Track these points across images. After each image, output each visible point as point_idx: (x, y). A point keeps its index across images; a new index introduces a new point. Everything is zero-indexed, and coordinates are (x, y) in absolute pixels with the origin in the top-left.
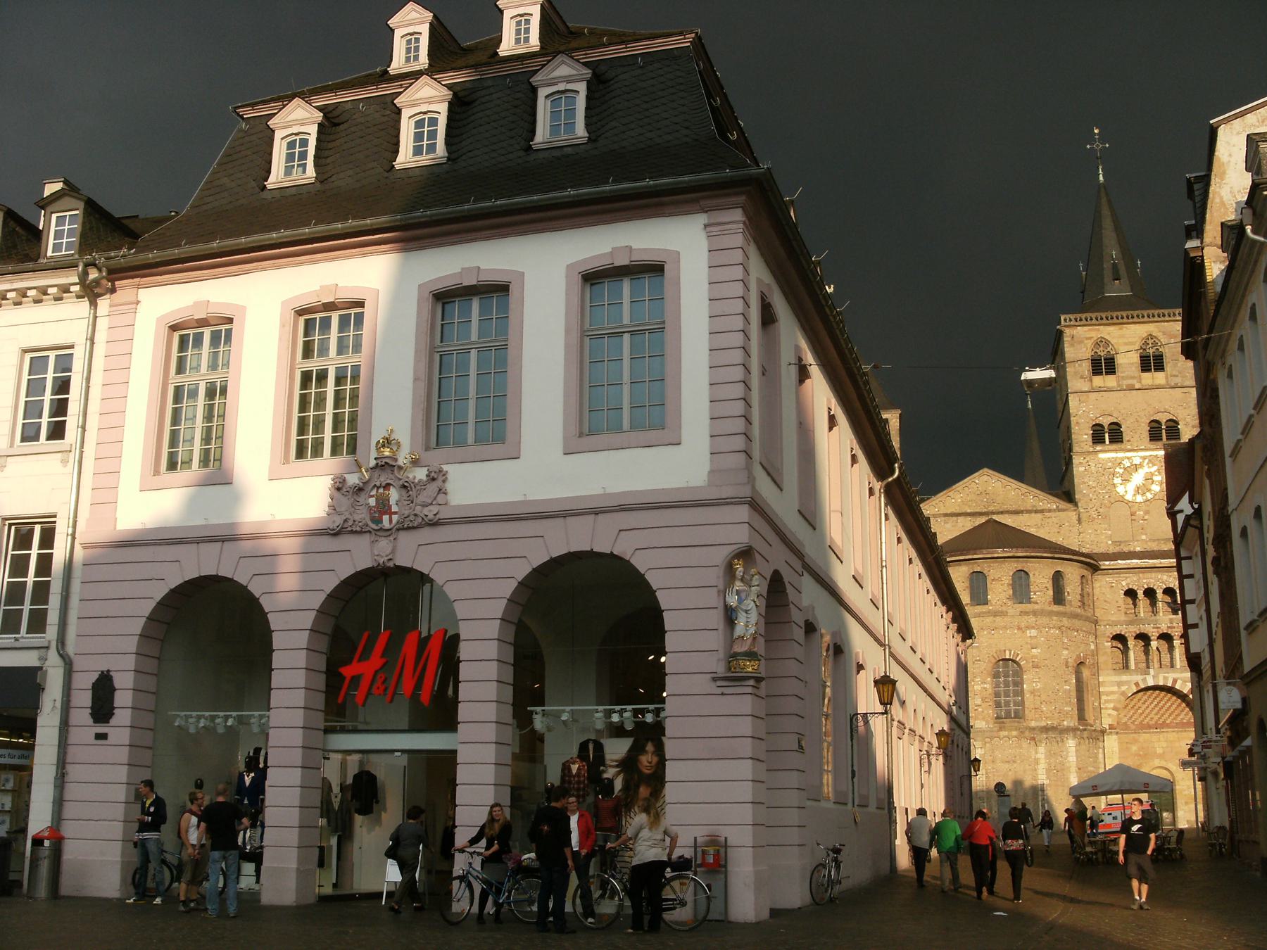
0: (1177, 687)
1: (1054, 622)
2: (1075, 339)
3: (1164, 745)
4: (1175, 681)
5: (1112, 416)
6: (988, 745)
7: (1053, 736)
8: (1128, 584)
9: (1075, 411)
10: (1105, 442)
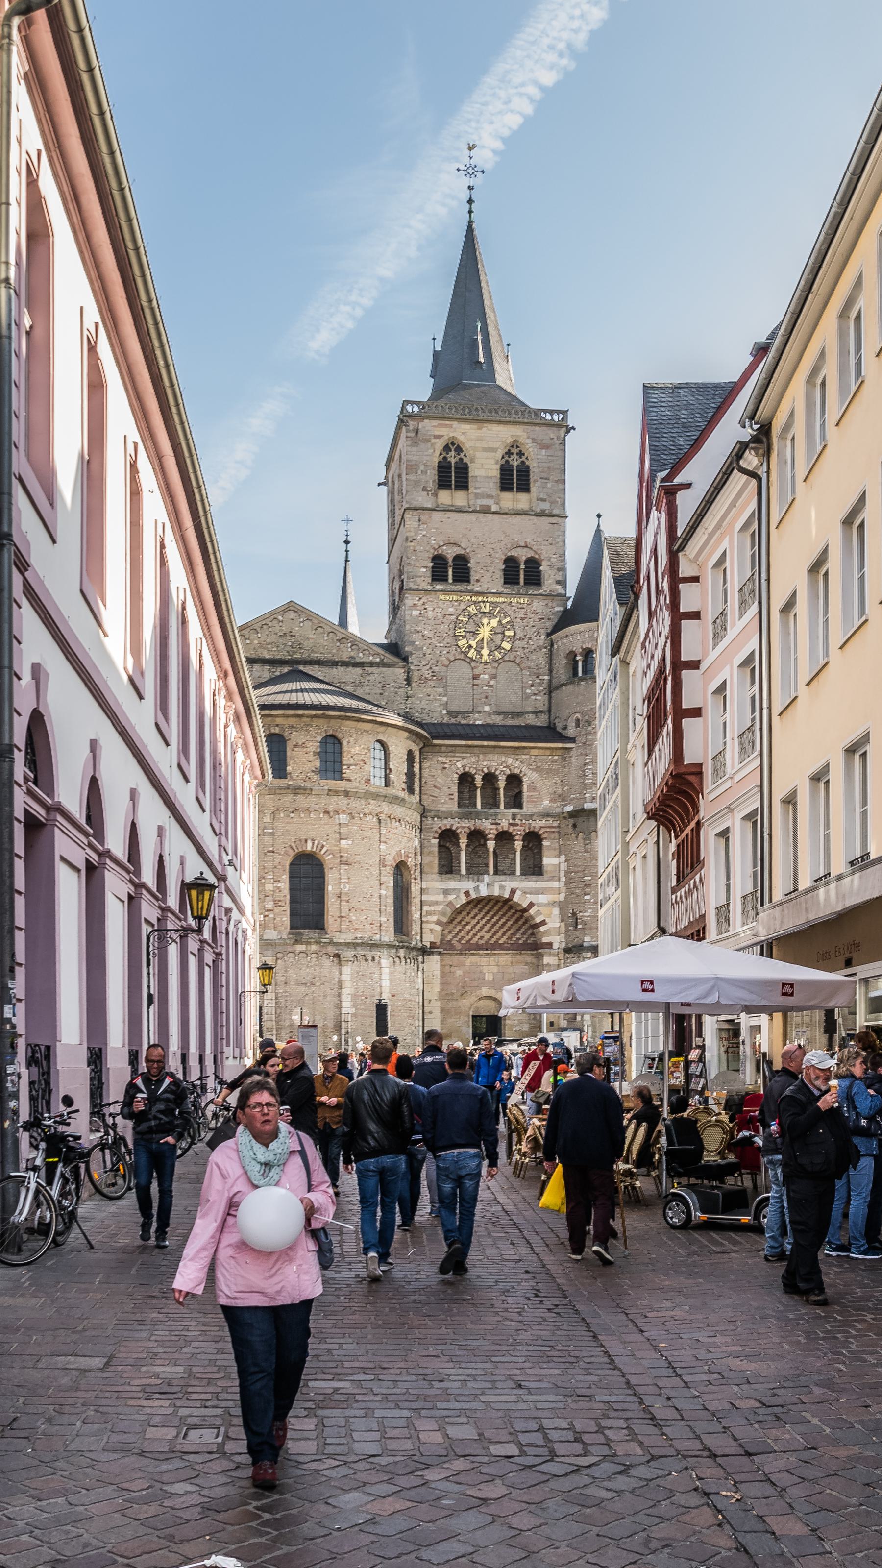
0: (516, 899)
2: (420, 435)
3: (495, 970)
4: (513, 892)
5: (459, 546)
6: (279, 961)
7: (363, 953)
8: (464, 766)
9: (412, 534)
10: (447, 580)
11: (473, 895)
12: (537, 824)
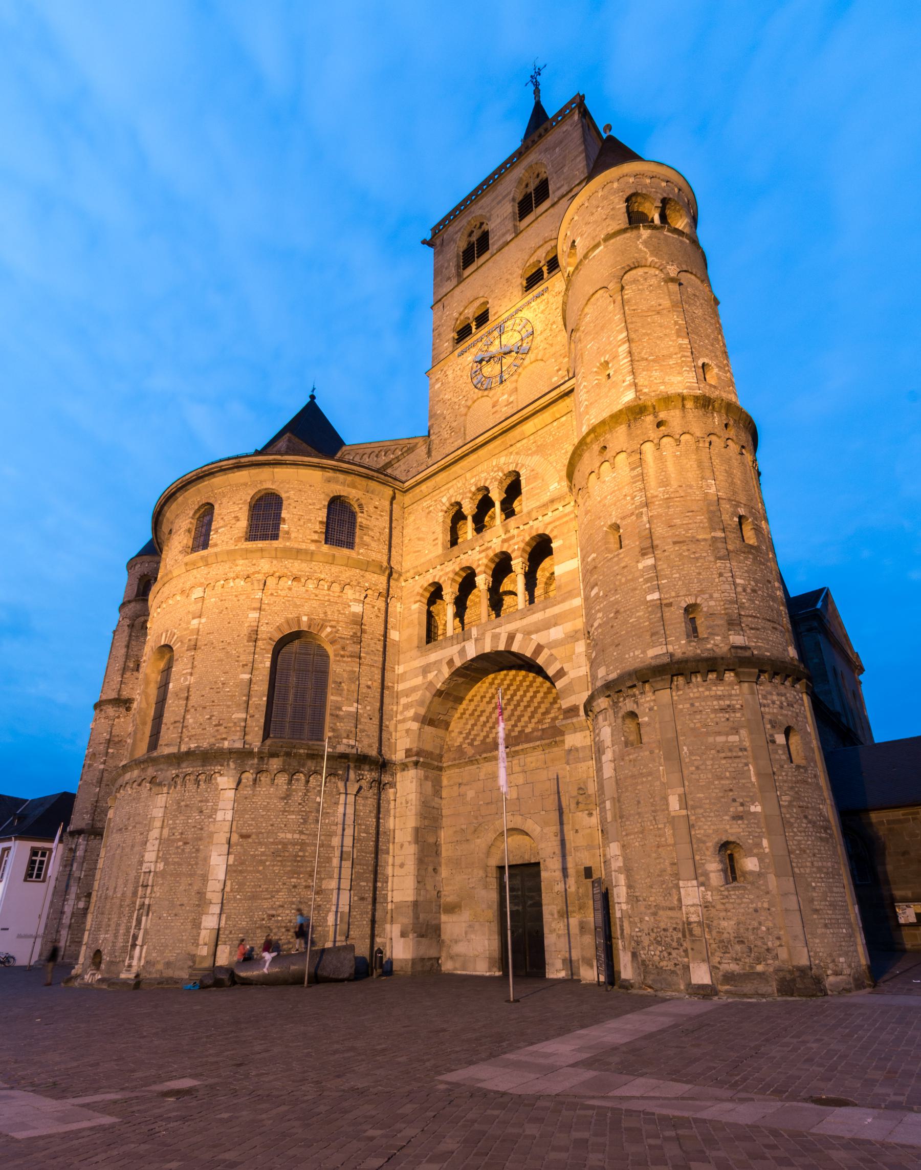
0: (515, 648)
1: (239, 568)
4: (511, 638)
8: (449, 499)
11: (458, 663)
12: (539, 526)
